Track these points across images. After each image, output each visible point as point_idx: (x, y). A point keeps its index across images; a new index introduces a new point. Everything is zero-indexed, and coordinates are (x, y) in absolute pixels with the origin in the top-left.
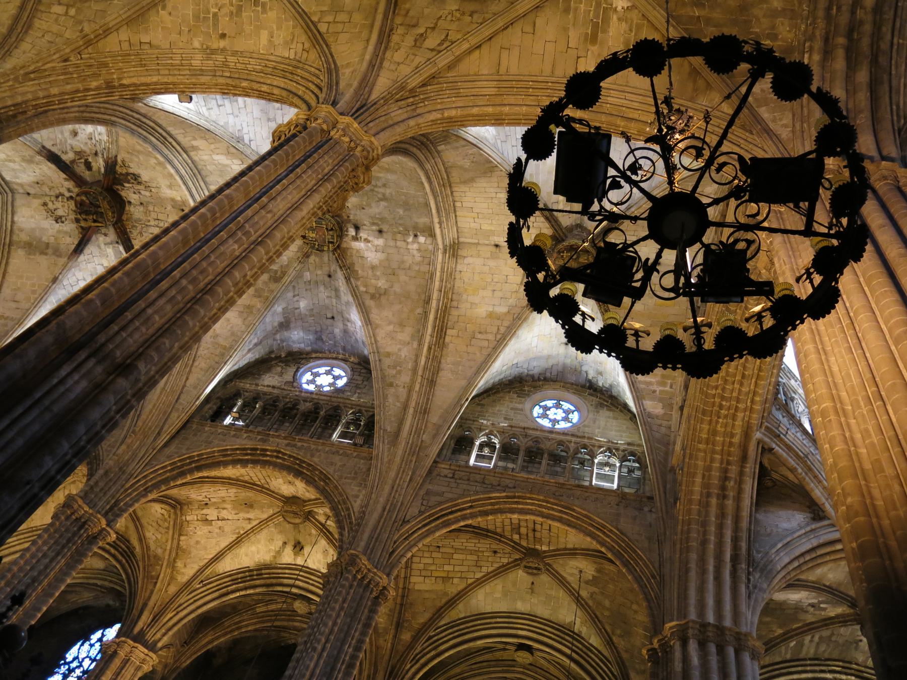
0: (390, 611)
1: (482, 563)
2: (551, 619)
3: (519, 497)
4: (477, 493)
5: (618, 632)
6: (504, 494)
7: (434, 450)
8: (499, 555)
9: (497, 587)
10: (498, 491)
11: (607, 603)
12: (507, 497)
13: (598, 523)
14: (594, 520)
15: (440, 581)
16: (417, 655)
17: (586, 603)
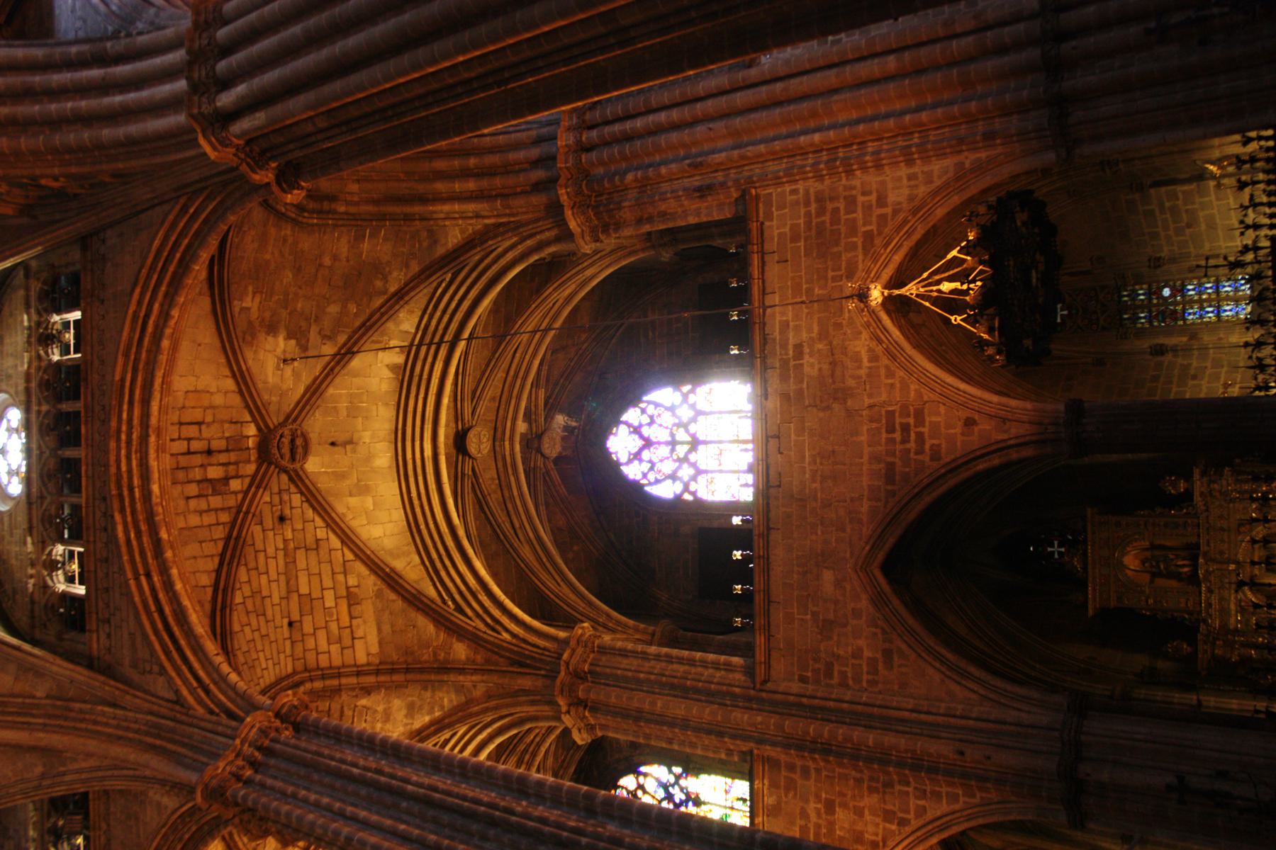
0: (425, 689)
1: (310, 540)
2: (394, 403)
3: (119, 487)
4: (122, 569)
5: (379, 284)
6: (118, 517)
7: (61, 668)
8: (287, 512)
9: (351, 508)
10: (114, 529)
11: (333, 309)
12: (122, 510)
13: (133, 330)
14: (130, 339)
15: (357, 610)
16: (487, 625)
17: (344, 345)
